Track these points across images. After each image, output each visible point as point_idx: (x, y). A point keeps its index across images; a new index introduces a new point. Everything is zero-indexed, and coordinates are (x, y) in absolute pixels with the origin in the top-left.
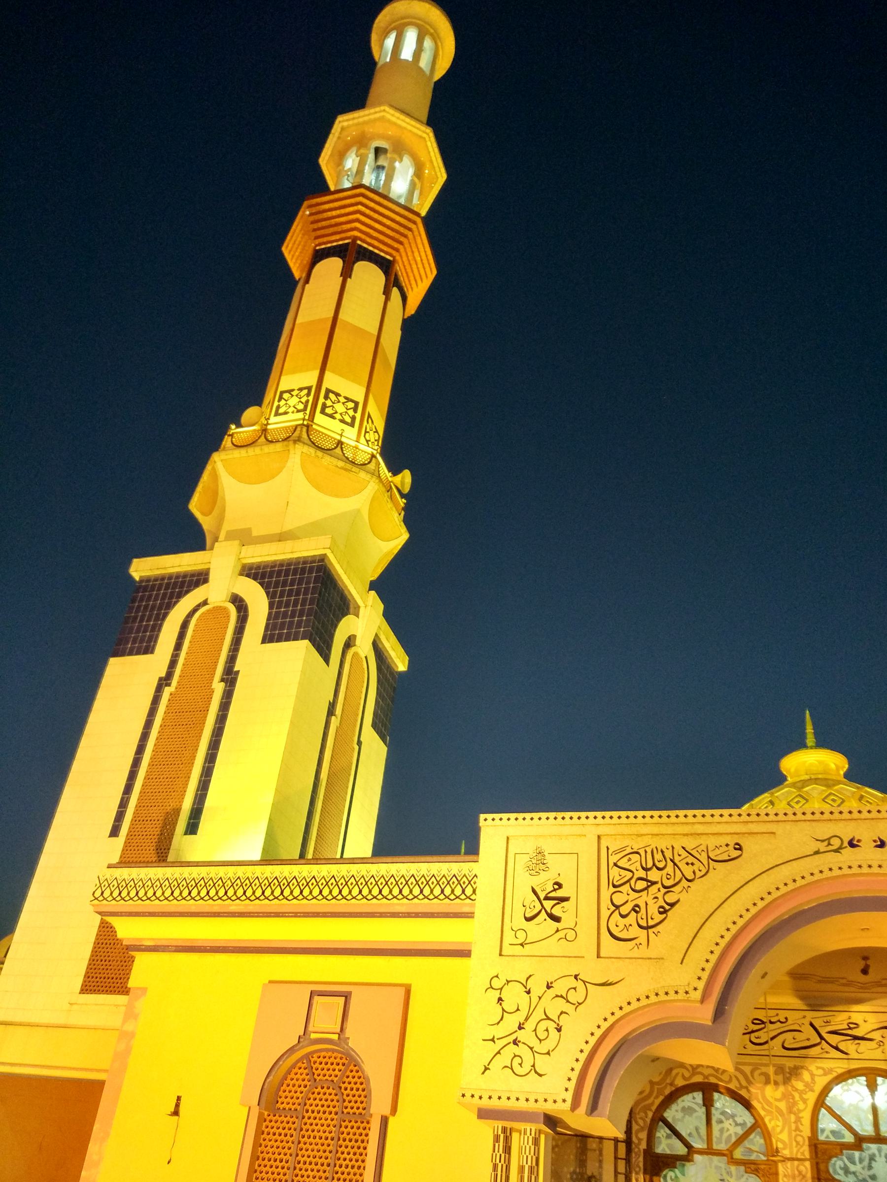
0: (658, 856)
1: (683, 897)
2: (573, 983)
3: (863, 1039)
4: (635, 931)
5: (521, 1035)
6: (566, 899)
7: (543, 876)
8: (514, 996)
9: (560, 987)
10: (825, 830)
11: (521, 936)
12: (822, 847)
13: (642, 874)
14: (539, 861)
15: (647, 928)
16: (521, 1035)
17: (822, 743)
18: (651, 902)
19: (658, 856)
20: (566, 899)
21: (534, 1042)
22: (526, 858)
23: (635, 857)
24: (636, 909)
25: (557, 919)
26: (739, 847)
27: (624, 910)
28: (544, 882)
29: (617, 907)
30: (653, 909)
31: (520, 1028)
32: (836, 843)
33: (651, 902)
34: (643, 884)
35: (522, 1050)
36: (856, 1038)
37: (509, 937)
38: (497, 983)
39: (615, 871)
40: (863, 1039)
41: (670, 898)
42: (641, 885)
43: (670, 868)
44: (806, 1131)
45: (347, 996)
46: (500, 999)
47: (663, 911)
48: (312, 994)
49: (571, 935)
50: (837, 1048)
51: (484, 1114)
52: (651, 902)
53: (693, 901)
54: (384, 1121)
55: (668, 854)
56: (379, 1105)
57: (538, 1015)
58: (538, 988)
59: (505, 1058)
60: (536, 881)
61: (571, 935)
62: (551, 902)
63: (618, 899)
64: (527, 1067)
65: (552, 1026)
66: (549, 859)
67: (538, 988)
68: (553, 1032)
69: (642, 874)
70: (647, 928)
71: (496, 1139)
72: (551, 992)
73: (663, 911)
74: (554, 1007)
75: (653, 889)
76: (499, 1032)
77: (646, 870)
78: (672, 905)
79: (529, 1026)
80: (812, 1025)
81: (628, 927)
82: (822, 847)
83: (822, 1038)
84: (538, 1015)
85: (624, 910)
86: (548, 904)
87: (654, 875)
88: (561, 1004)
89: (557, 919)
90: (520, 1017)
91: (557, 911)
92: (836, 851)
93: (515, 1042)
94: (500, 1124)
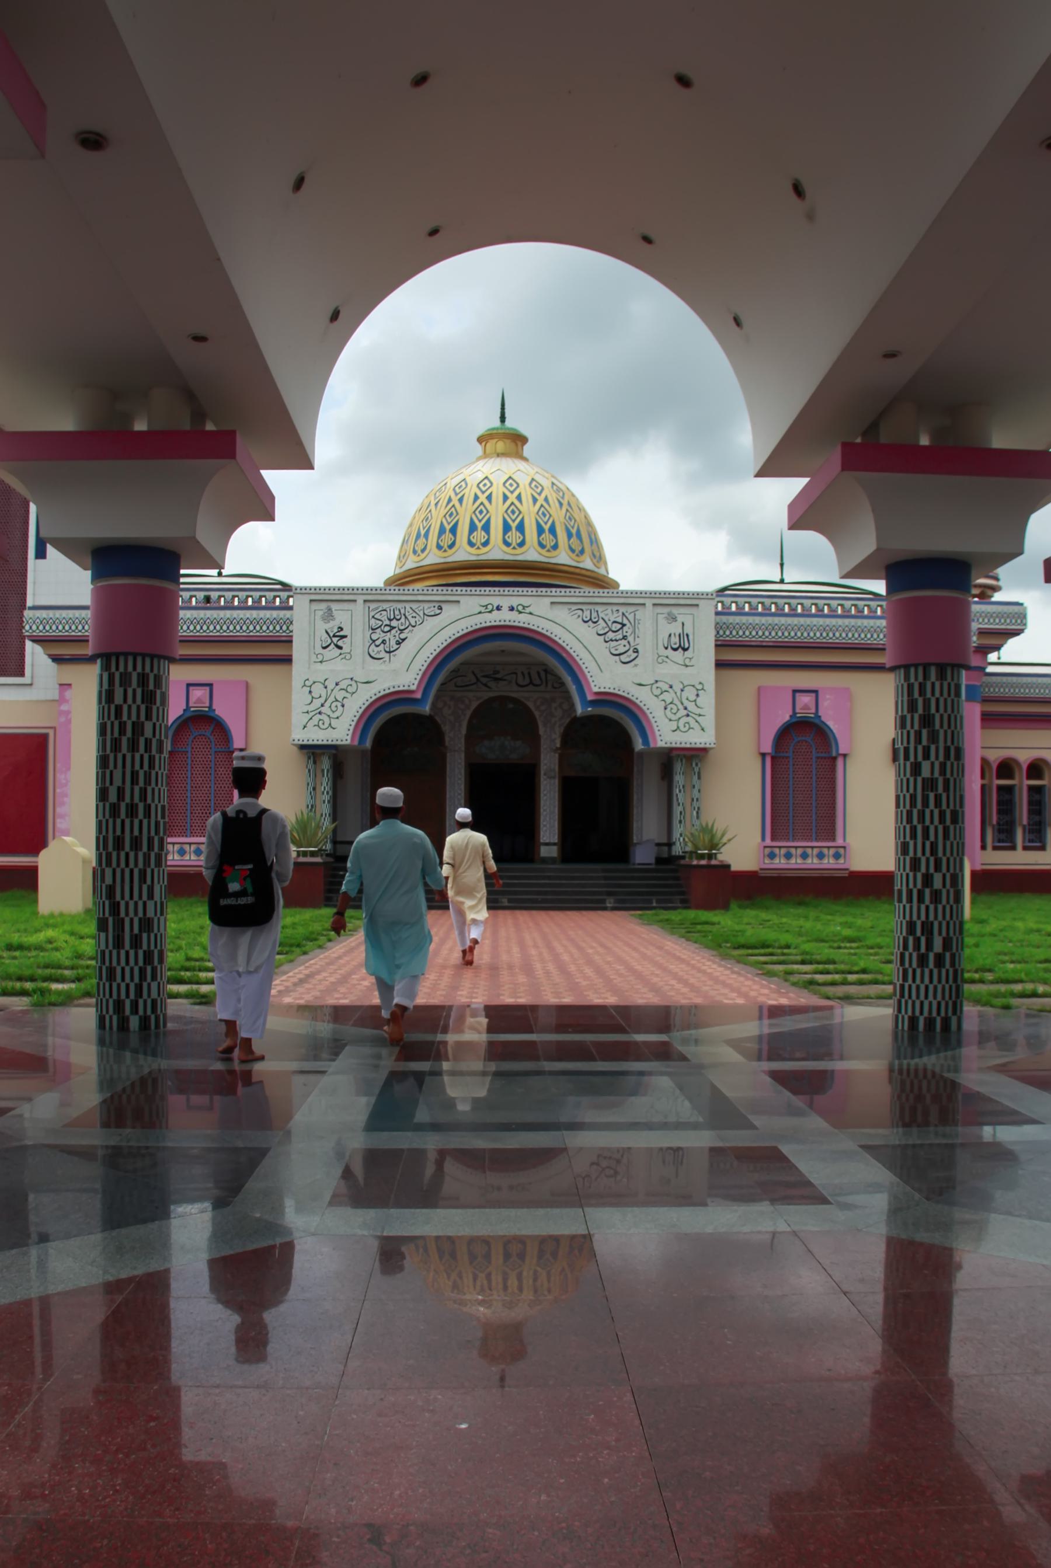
0: (397, 612)
1: (409, 635)
2: (350, 682)
3: (501, 679)
4: (383, 654)
5: (323, 709)
6: (345, 637)
7: (332, 624)
8: (318, 690)
10: (485, 601)
11: (320, 658)
12: (483, 609)
13: (388, 622)
15: (390, 652)
16: (323, 709)
18: (392, 638)
19: (397, 612)
20: (345, 637)
21: (330, 713)
22: (321, 613)
23: (384, 613)
24: (384, 642)
25: (340, 648)
27: (377, 643)
28: (332, 626)
29: (374, 641)
30: (393, 642)
31: (322, 705)
32: (490, 607)
33: (392, 638)
34: (387, 629)
36: (496, 679)
38: (308, 683)
39: (373, 621)
40: (501, 679)
41: (403, 636)
42: (387, 629)
43: (403, 620)
44: (464, 731)
46: (310, 692)
49: (348, 657)
50: (485, 685)
52: (392, 638)
53: (414, 639)
55: (402, 611)
57: (332, 699)
60: (327, 626)
61: (348, 657)
63: (374, 637)
64: (327, 725)
65: (339, 704)
66: (335, 613)
67: (331, 685)
68: (340, 708)
69: (388, 622)
70: (390, 652)
72: (338, 687)
73: (398, 643)
74: (340, 695)
75: (393, 631)
76: (311, 708)
77: (390, 620)
78: (403, 640)
79: (327, 704)
80: (473, 673)
81: (379, 651)
82: (483, 609)
83: (478, 680)
84: (332, 699)
85: (377, 643)
86: (335, 640)
87: (394, 623)
88: (344, 693)
89: (340, 648)
90: (322, 700)
91: (340, 643)
92: (490, 612)
93: (320, 713)
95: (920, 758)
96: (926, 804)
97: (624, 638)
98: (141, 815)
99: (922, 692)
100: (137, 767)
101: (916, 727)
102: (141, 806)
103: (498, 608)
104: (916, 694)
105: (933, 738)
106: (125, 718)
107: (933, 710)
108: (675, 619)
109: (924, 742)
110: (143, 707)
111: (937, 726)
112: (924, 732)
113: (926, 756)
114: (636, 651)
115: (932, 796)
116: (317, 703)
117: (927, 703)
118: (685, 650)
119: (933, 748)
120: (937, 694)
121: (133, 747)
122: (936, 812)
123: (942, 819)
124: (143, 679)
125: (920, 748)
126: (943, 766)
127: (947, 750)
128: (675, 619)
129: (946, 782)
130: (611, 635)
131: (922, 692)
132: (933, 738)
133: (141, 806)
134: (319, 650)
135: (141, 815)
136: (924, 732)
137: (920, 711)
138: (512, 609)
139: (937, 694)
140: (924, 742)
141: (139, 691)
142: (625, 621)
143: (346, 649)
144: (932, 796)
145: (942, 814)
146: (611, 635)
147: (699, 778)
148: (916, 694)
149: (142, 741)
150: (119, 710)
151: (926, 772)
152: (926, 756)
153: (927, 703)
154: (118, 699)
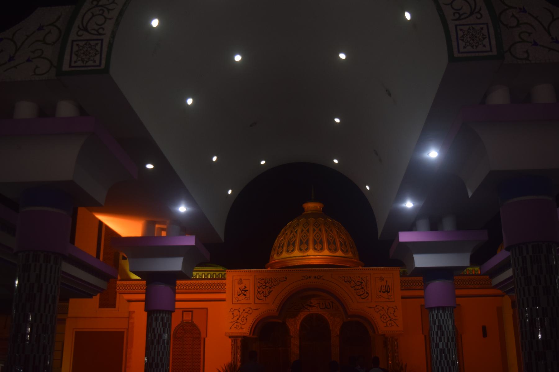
2: (249, 309)
4: (263, 297)
5: (238, 321)
7: (242, 285)
8: (236, 313)
9: (246, 310)
14: (241, 282)
16: (238, 321)
17: (315, 200)
24: (263, 292)
25: (245, 295)
26: (286, 278)
28: (242, 286)
30: (267, 292)
35: (239, 324)
37: (234, 300)
39: (258, 284)
41: (271, 290)
44: (298, 328)
45: (192, 312)
47: (269, 293)
48: (183, 311)
51: (230, 337)
54: (204, 339)
56: (203, 335)
57: (242, 316)
58: (241, 311)
59: (235, 326)
60: (240, 286)
62: (244, 291)
63: (259, 290)
67: (241, 311)
71: (232, 341)
78: (271, 291)
79: (240, 319)
84: (242, 316)
86: (243, 292)
87: (267, 285)
89: (245, 295)
90: (238, 317)
91: (245, 293)
94: (233, 339)
95: (438, 341)
96: (441, 358)
97: (362, 288)
98: (160, 367)
99: (437, 317)
100: (159, 350)
101: (436, 330)
102: (160, 364)
103: (310, 277)
104: (435, 318)
105: (442, 334)
106: (156, 332)
107: (442, 323)
108: (383, 279)
109: (439, 335)
110: (162, 329)
111: (444, 329)
112: (439, 332)
113: (440, 341)
114: (368, 293)
115: (443, 355)
116: (236, 318)
117: (439, 321)
118: (388, 292)
119: (443, 338)
120: (443, 318)
121: (158, 343)
122: (446, 361)
123: (448, 364)
124: (162, 319)
125: (438, 338)
126: (447, 344)
127: (448, 338)
128: (383, 279)
129: (449, 350)
130: (357, 287)
131: (437, 317)
132: (442, 334)
133: (160, 364)
134: (236, 296)
135: (160, 367)
136: (439, 332)
137: (437, 324)
138: (315, 278)
139: (443, 318)
140: (439, 335)
141: (161, 323)
142: (363, 281)
143: (248, 295)
144: (443, 355)
145: (448, 362)
146: (357, 287)
147: (397, 347)
148: (435, 318)
149: (161, 340)
150: (154, 329)
151: (441, 346)
152: (440, 341)
153: (439, 321)
154: (154, 326)
